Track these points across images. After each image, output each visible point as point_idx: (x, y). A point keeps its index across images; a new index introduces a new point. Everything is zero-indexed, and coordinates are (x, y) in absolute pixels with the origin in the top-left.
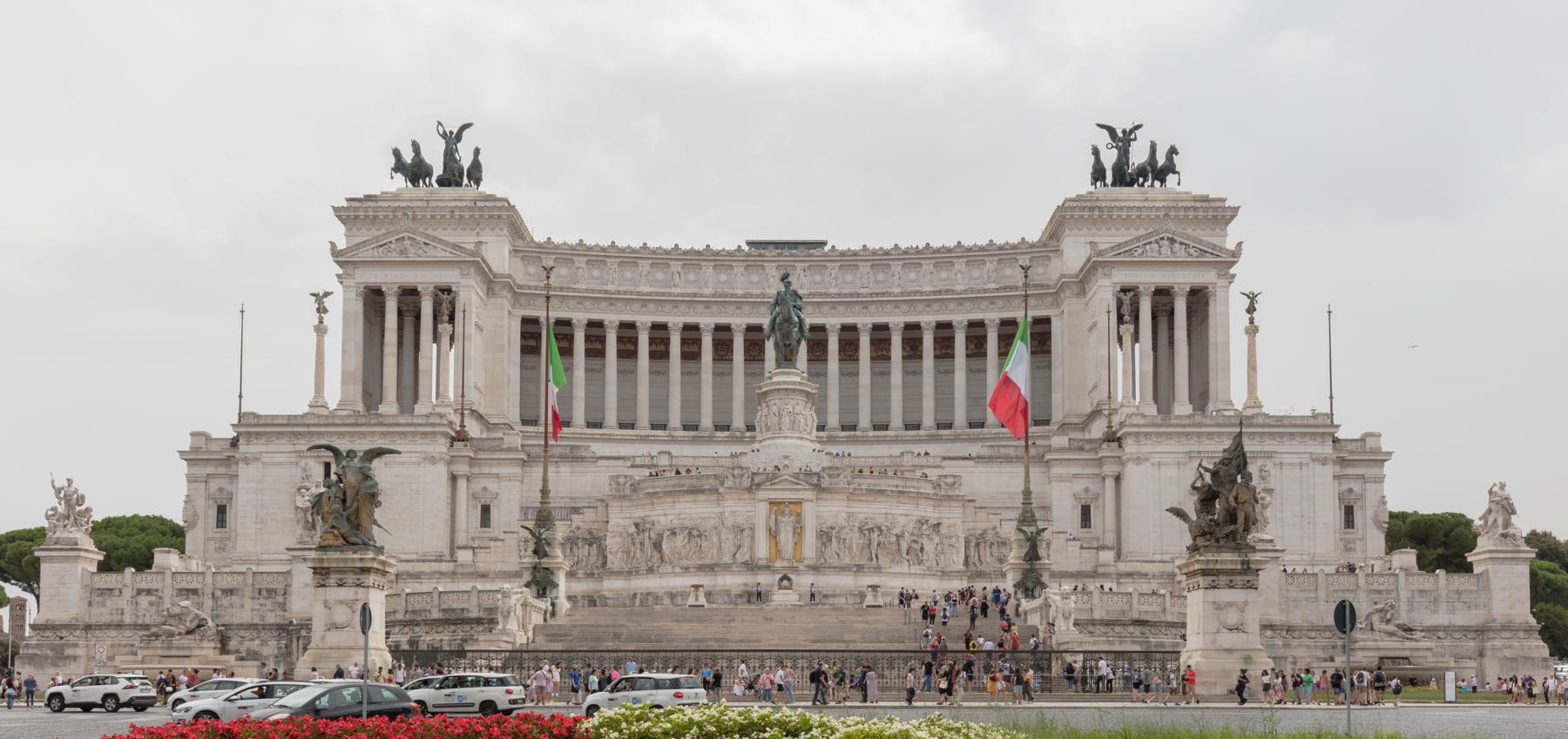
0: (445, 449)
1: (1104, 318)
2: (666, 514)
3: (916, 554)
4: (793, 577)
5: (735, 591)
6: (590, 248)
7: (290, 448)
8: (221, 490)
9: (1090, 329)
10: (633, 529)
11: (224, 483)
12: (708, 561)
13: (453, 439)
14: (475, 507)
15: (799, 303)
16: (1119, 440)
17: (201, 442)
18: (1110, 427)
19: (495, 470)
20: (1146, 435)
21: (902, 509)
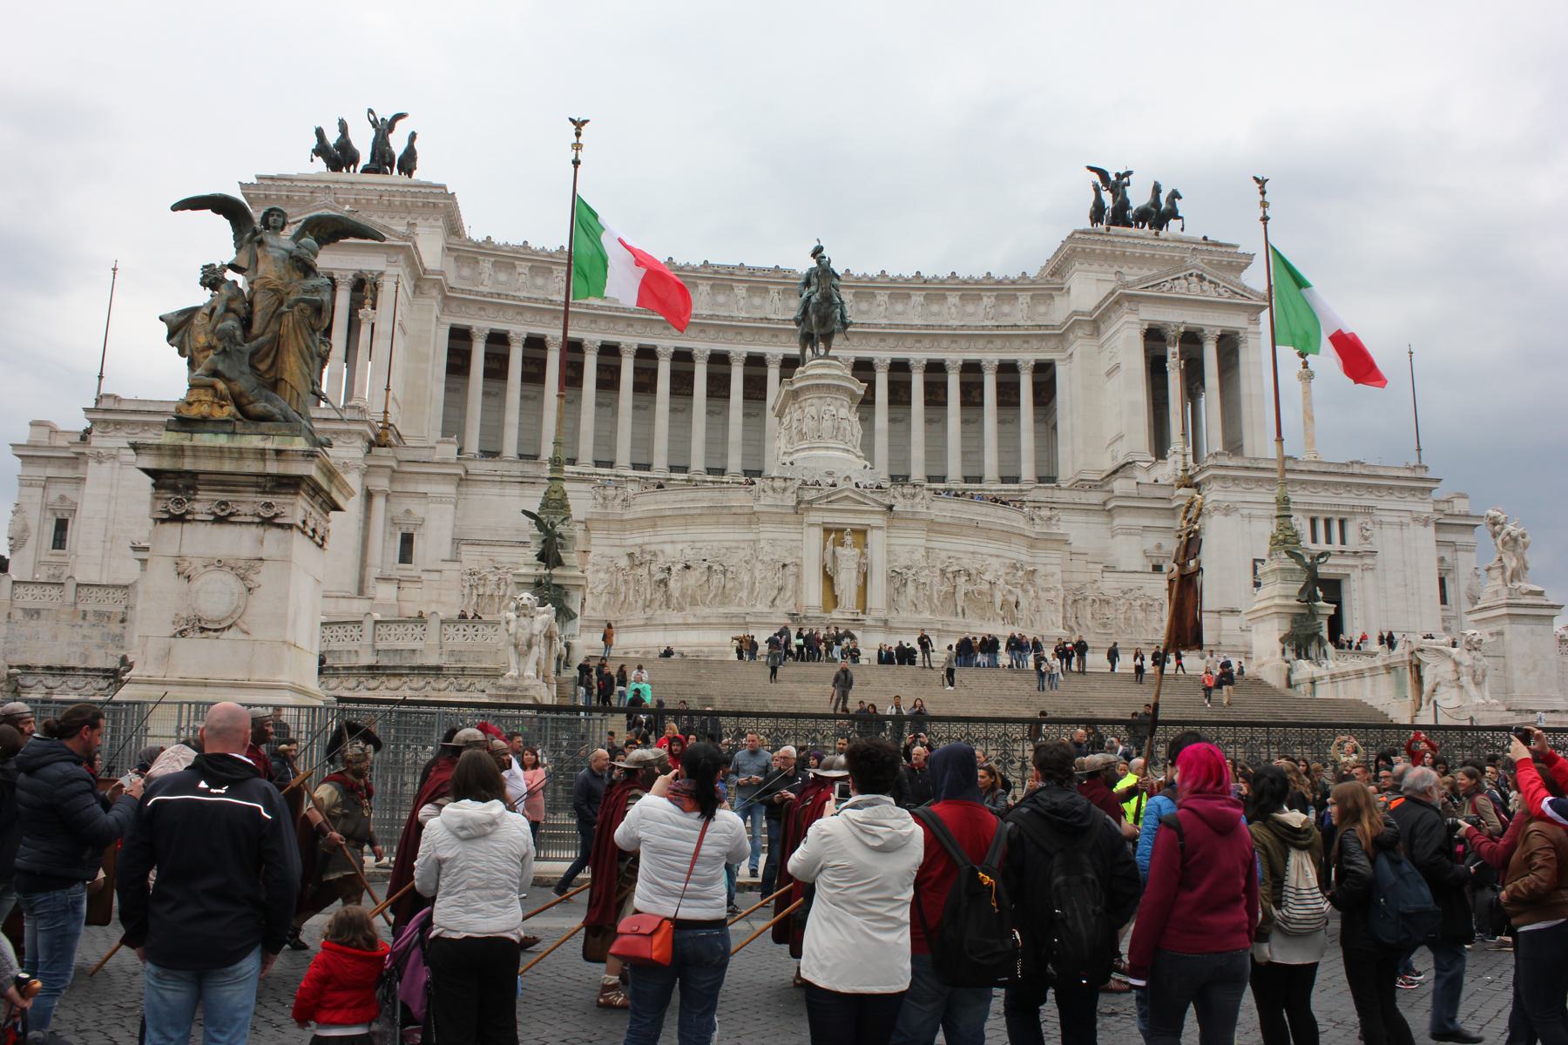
0: (360, 454)
2: (673, 545)
4: (857, 633)
6: (535, 253)
8: (63, 498)
9: (1109, 374)
10: (624, 562)
12: (733, 609)
13: (372, 444)
14: (393, 535)
15: (835, 281)
16: (1197, 486)
17: (42, 437)
18: (1185, 470)
19: (422, 488)
20: (1235, 479)
21: (991, 547)
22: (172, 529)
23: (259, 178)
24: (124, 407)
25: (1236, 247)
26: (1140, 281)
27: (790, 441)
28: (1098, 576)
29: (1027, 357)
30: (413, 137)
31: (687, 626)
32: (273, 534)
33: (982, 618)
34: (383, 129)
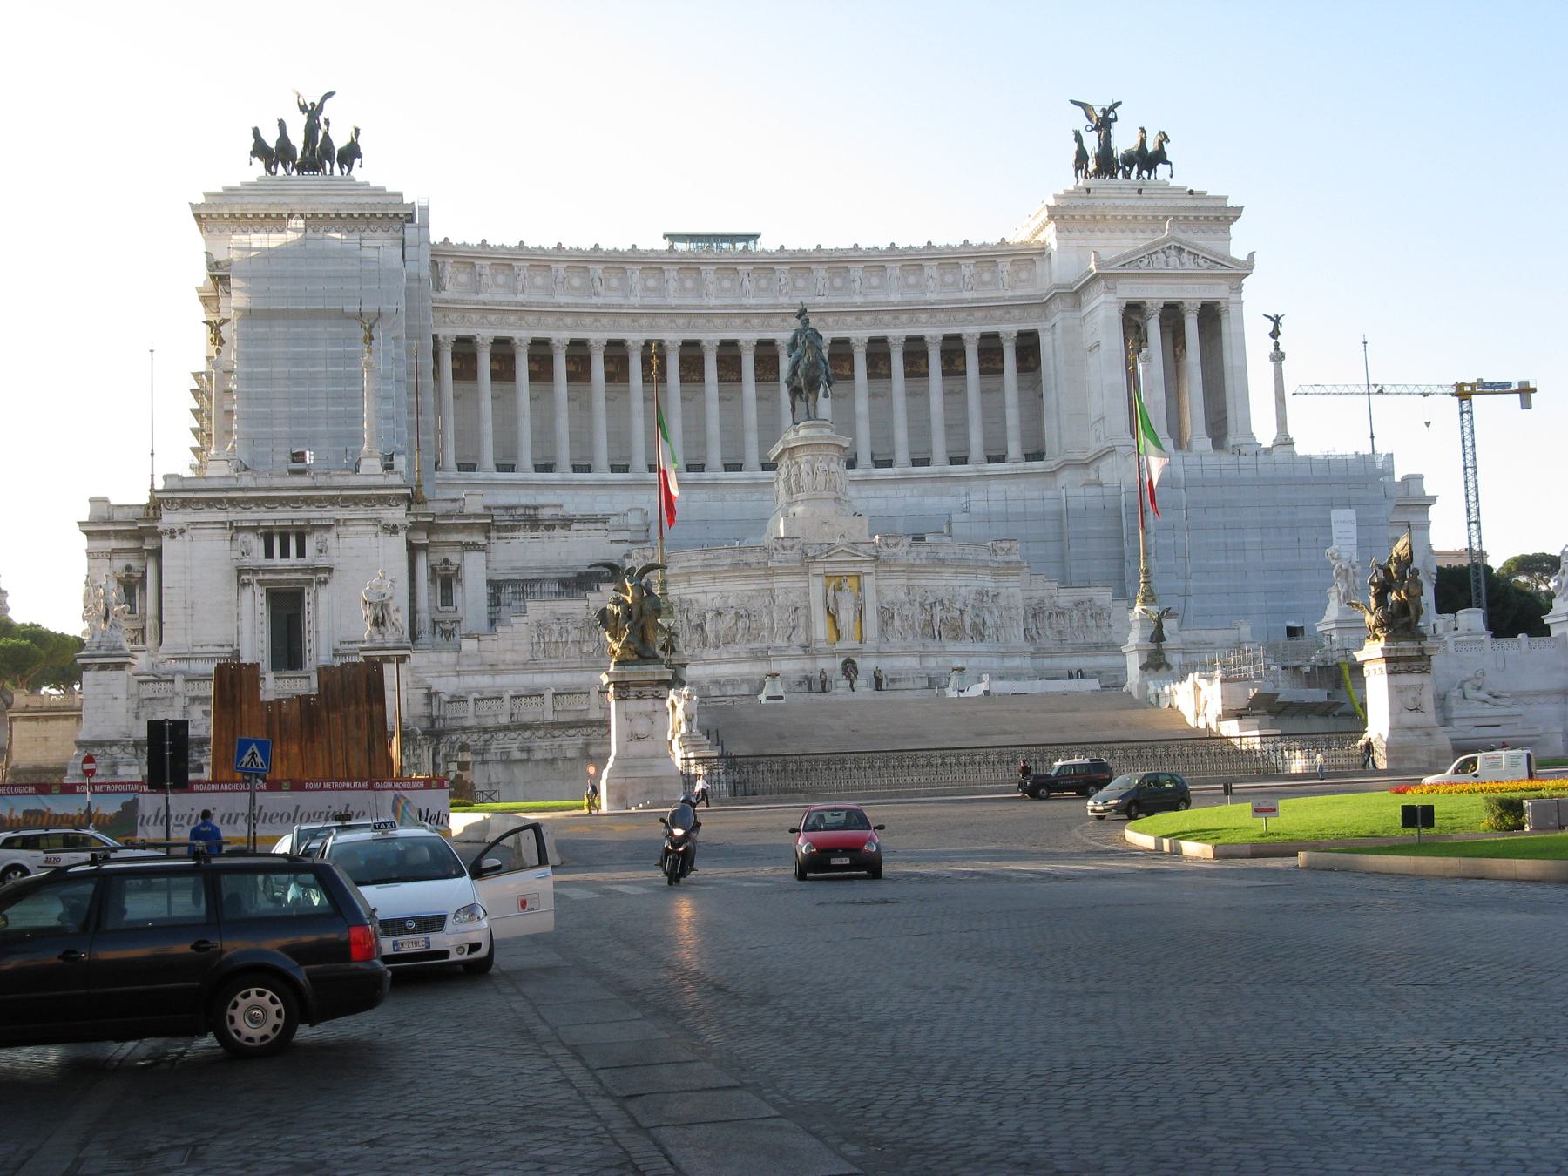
1: (1111, 337)
3: (979, 631)
5: (796, 678)
7: (222, 516)
8: (128, 568)
11: (135, 564)
12: (756, 645)
21: (961, 580)
22: (622, 703)
23: (207, 195)
24: (188, 485)
25: (1226, 198)
26: (1117, 259)
27: (789, 492)
28: (1054, 592)
29: (1009, 329)
30: (357, 131)
31: (720, 661)
32: (658, 702)
33: (955, 638)
34: (313, 113)
